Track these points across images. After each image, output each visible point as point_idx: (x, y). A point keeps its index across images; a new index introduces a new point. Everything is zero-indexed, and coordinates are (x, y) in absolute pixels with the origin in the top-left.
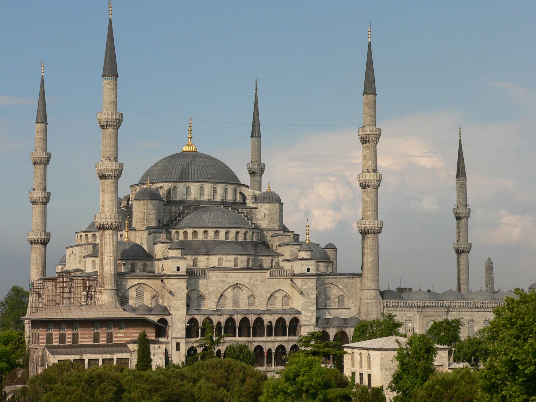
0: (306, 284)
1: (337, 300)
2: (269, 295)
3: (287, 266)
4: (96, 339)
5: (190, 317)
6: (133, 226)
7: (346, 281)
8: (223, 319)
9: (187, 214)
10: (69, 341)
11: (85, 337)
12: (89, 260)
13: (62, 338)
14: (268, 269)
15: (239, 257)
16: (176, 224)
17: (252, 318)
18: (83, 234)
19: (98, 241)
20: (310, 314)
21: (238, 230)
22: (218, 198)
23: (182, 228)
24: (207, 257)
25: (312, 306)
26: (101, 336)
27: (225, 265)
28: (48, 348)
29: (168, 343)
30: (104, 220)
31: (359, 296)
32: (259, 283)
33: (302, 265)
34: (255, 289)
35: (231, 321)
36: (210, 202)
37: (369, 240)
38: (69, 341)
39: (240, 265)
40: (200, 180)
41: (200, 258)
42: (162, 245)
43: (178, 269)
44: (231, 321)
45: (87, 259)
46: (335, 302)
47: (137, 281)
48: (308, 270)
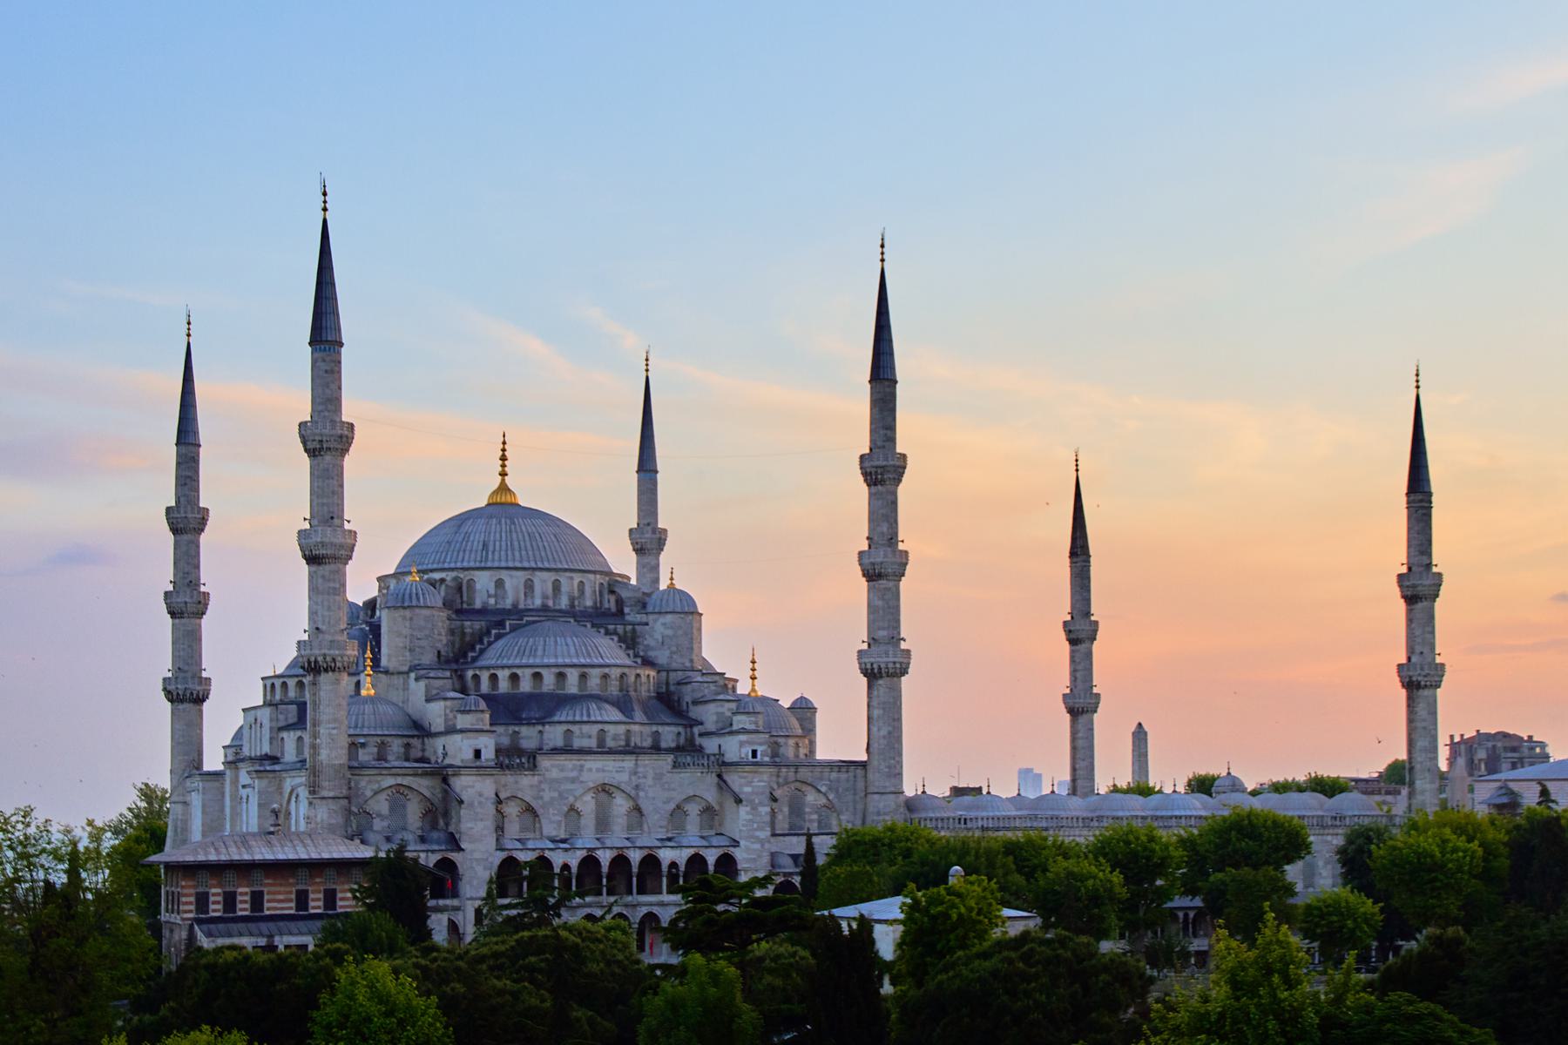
0: (749, 784)
1: (815, 817)
2: (672, 806)
3: (710, 745)
4: (302, 900)
5: (503, 855)
6: (384, 662)
7: (834, 775)
8: (574, 861)
9: (499, 637)
10: (243, 908)
11: (279, 901)
12: (290, 738)
13: (230, 901)
14: (669, 751)
15: (606, 727)
16: (474, 659)
17: (635, 857)
18: (278, 683)
19: (308, 697)
20: (757, 846)
21: (606, 670)
22: (564, 603)
23: (488, 668)
24: (540, 728)
25: (760, 829)
26: (311, 896)
27: (577, 744)
28: (199, 921)
29: (457, 909)
30: (317, 652)
31: (860, 806)
32: (650, 781)
33: (742, 744)
34: (642, 794)
35: (590, 862)
36: (545, 608)
37: (882, 690)
38: (243, 908)
39: (610, 743)
40: (526, 565)
41: (525, 731)
42: (442, 703)
43: (478, 754)
44: (590, 862)
45: (285, 734)
46: (811, 821)
47: (391, 781)
48: (754, 753)
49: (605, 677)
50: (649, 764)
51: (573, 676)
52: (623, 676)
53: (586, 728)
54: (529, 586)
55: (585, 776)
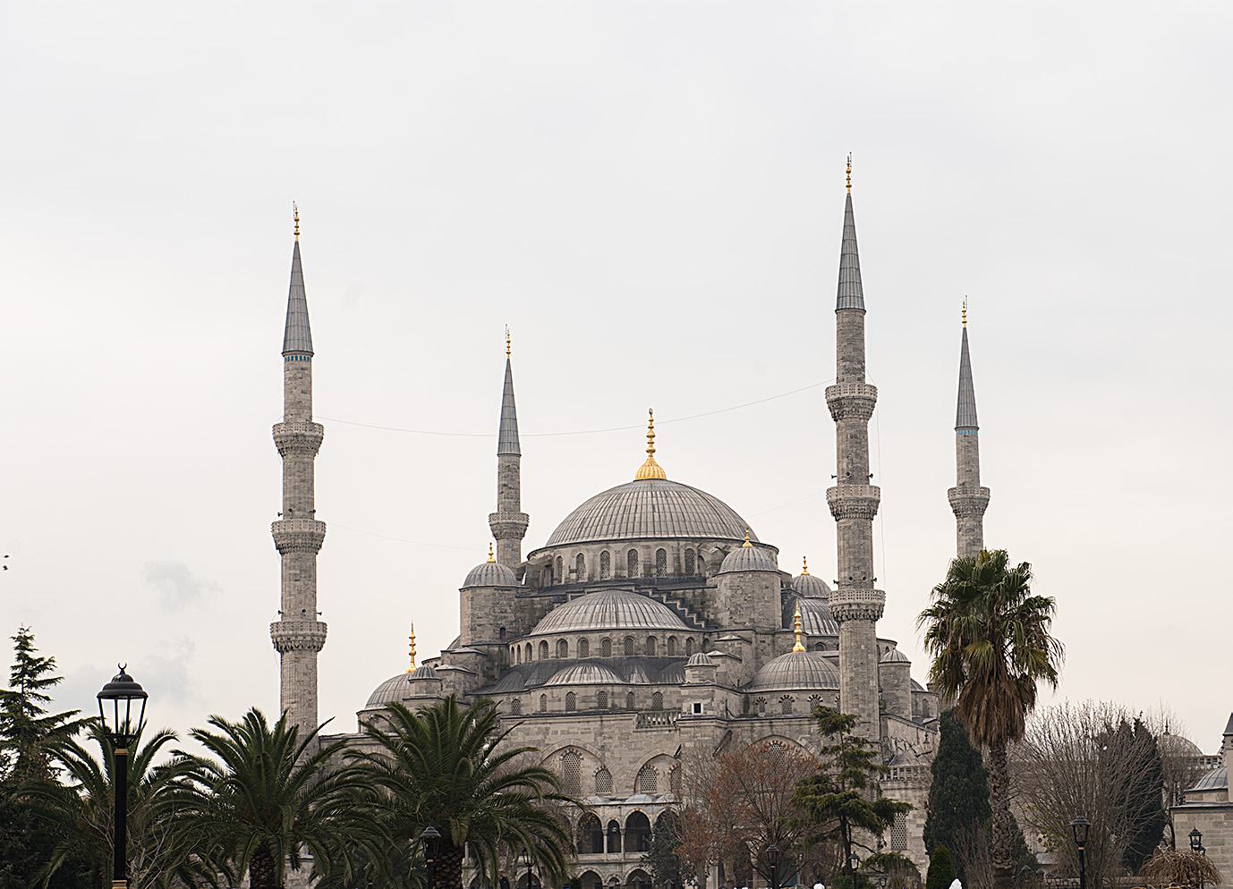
15: (575, 690)
21: (607, 634)
22: (640, 571)
32: (616, 741)
39: (579, 705)
49: (607, 641)
50: (619, 727)
51: (573, 642)
52: (628, 639)
53: (556, 691)
54: (605, 558)
55: (551, 739)
